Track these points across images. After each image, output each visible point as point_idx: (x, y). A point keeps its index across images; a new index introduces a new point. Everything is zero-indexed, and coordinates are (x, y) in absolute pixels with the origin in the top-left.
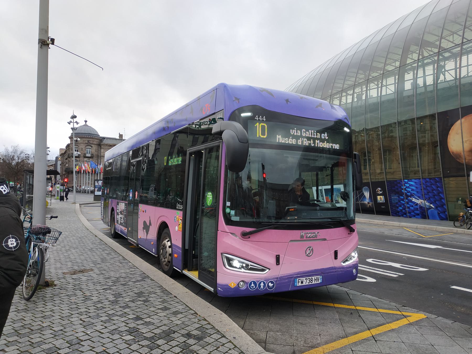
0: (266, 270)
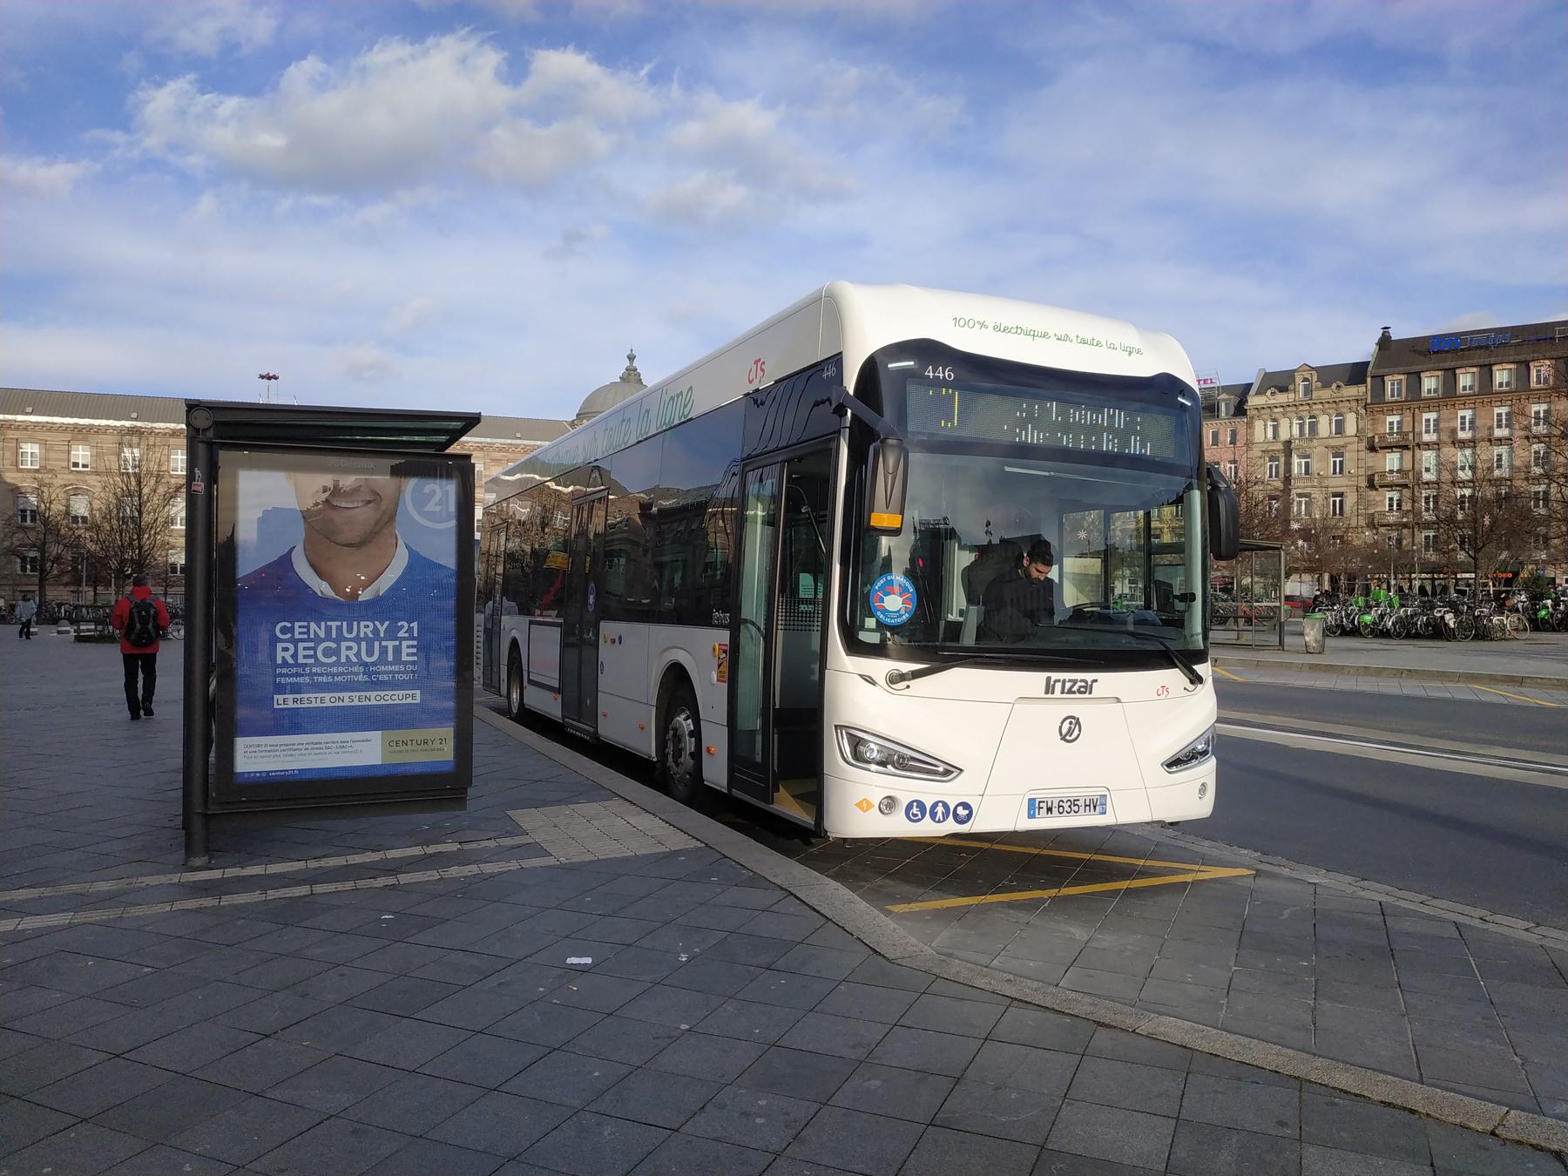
0: (953, 772)
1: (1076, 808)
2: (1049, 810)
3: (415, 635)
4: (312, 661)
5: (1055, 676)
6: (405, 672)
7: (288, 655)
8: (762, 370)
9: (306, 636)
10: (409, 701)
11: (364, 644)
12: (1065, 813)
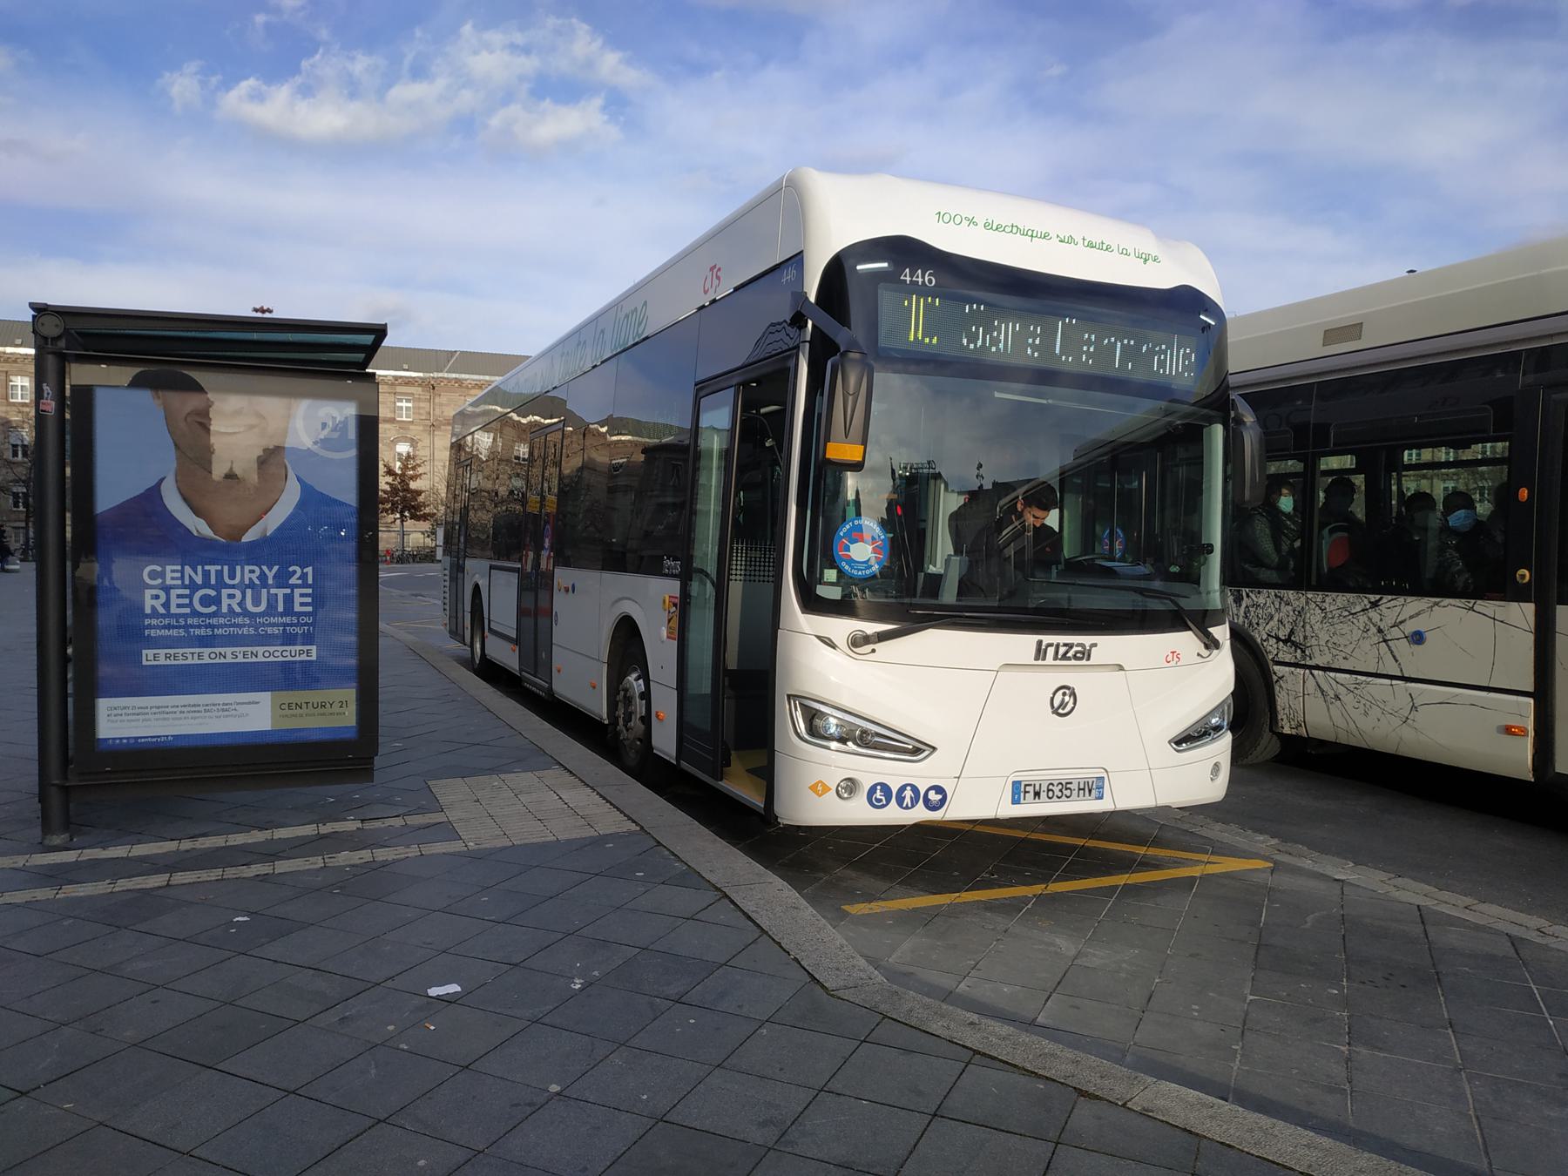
0: (924, 751)
1: (1068, 793)
2: (1037, 794)
3: (310, 581)
4: (187, 610)
5: (1047, 639)
6: (298, 624)
7: (158, 604)
8: (718, 278)
9: (179, 582)
10: (304, 657)
11: (249, 592)
12: (1055, 799)
